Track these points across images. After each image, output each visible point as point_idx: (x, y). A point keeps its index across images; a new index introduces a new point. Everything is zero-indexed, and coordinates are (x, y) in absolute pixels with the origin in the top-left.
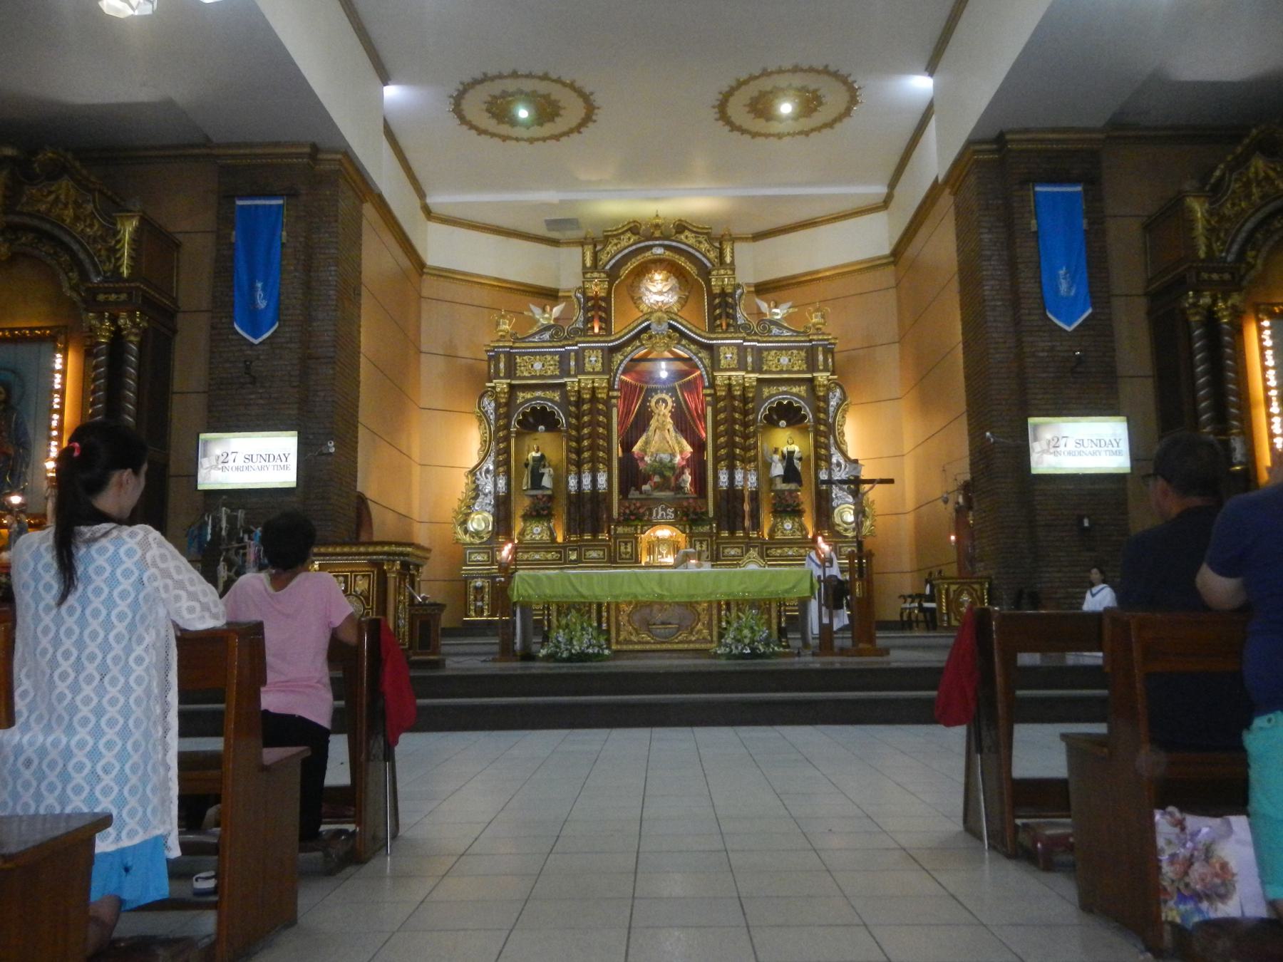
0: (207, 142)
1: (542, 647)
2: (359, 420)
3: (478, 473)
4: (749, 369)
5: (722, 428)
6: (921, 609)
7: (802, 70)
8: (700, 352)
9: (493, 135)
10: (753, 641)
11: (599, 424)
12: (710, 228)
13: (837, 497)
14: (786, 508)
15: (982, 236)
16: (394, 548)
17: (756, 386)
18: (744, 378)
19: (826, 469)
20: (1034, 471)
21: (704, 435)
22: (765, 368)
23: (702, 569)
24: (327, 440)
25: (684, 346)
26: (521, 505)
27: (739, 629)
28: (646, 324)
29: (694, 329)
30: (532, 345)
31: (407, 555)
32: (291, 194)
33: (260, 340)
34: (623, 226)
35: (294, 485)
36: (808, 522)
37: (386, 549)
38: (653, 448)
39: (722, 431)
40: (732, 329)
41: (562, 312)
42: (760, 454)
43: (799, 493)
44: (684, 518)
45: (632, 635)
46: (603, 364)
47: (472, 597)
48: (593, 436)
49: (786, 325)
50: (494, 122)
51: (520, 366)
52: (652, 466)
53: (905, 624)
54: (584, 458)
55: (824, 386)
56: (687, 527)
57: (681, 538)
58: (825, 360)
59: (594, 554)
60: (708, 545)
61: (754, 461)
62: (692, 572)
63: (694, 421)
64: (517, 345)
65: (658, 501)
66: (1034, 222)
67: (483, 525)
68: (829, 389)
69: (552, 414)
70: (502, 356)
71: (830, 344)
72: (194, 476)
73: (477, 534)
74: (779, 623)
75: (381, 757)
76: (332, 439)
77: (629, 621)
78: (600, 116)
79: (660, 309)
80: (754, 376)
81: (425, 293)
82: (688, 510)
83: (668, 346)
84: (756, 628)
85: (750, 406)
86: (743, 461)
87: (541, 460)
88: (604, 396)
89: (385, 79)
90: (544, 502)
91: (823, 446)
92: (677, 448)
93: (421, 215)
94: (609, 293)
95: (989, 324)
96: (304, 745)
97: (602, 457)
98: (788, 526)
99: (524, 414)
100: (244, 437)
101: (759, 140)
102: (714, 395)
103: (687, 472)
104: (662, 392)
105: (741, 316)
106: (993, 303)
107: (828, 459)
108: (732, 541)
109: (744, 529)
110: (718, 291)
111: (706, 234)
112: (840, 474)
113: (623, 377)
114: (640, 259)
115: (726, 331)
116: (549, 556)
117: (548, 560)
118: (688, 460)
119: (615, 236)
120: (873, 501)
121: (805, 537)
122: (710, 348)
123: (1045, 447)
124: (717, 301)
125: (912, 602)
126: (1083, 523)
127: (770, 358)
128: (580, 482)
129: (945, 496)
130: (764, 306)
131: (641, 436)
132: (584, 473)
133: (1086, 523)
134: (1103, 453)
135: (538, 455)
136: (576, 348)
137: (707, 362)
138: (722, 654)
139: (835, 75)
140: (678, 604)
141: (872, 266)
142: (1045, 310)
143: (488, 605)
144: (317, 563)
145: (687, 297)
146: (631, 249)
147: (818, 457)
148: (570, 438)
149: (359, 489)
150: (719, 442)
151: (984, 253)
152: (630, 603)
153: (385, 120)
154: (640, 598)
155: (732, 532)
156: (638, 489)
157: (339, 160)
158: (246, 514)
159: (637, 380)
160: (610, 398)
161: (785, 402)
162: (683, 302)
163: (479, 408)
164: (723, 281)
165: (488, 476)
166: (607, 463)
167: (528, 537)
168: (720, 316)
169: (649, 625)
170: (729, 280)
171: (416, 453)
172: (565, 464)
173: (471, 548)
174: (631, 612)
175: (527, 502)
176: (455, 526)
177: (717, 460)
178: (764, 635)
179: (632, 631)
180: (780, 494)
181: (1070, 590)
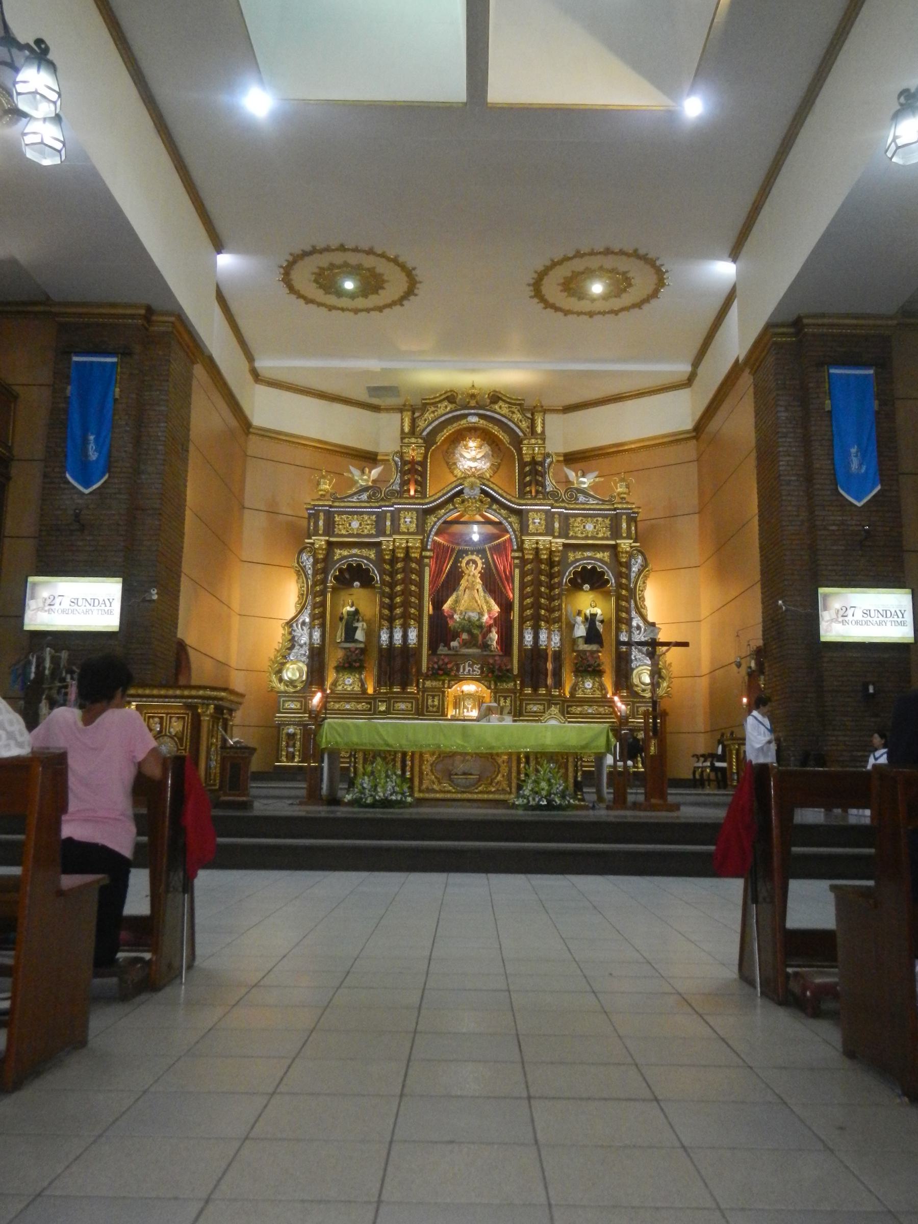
0: (47, 301)
1: (348, 793)
2: (183, 570)
3: (294, 625)
4: (556, 534)
5: (529, 589)
6: (713, 767)
7: (613, 253)
8: (510, 518)
9: (320, 304)
10: (549, 794)
11: (412, 582)
12: (523, 400)
13: (636, 659)
15: (779, 414)
16: (209, 693)
17: (562, 551)
18: (551, 543)
19: (626, 632)
20: (823, 639)
21: (511, 596)
22: (571, 533)
23: (503, 723)
24: (150, 588)
25: (495, 510)
26: (334, 657)
27: (536, 782)
28: (459, 488)
29: (505, 495)
30: (351, 504)
31: (221, 699)
32: (125, 353)
34: (441, 395)
35: (116, 629)
36: (608, 681)
37: (201, 693)
38: (463, 606)
39: (528, 593)
41: (380, 475)
42: (564, 617)
43: (600, 654)
44: (490, 675)
45: (434, 783)
46: (417, 525)
47: (284, 743)
48: (406, 593)
49: (592, 493)
50: (321, 292)
51: (338, 525)
52: (460, 623)
53: (697, 782)
54: (397, 614)
55: (627, 552)
56: (493, 682)
57: (486, 693)
58: (629, 528)
59: (402, 706)
60: (511, 701)
61: (558, 622)
62: (493, 726)
63: (503, 584)
64: (336, 504)
65: (466, 657)
66: (828, 402)
67: (298, 675)
68: (631, 556)
69: (367, 571)
70: (322, 514)
71: (634, 513)
72: (20, 616)
73: (291, 683)
74: (576, 777)
75: (180, 889)
76: (155, 587)
77: (432, 771)
78: (421, 290)
79: (473, 475)
80: (561, 541)
81: (249, 452)
82: (494, 667)
83: (480, 510)
84: (553, 781)
85: (556, 569)
86: (547, 622)
89: (219, 247)
90: (357, 654)
91: (624, 609)
92: (485, 608)
93: (249, 378)
94: (425, 457)
95: (784, 498)
96: (103, 873)
97: (413, 614)
98: (589, 685)
99: (341, 570)
100: (72, 582)
101: (570, 317)
102: (522, 559)
103: (494, 630)
104: (472, 554)
105: (550, 483)
106: (788, 478)
107: (629, 621)
109: (546, 686)
110: (529, 460)
111: (520, 405)
112: (639, 636)
113: (436, 538)
114: (454, 427)
115: (535, 498)
116: (359, 707)
117: (359, 711)
118: (495, 619)
119: (433, 404)
120: (671, 663)
121: (605, 696)
122: (519, 513)
123: (834, 616)
124: (527, 469)
125: (705, 761)
126: (868, 690)
127: (576, 524)
128: (391, 637)
129: (738, 660)
130: (572, 475)
131: (451, 594)
132: (396, 628)
133: (871, 690)
134: (889, 624)
135: (353, 609)
136: (392, 509)
137: (516, 526)
138: (519, 805)
139: (644, 258)
140: (479, 755)
141: (676, 440)
142: (837, 485)
143: (299, 751)
144: (134, 703)
145: (499, 464)
146: (447, 416)
147: (619, 620)
148: (383, 594)
149: (180, 635)
150: (525, 603)
151: (780, 430)
152: (433, 754)
153: (218, 286)
154: (443, 749)
155: (535, 689)
156: (447, 645)
157: (172, 323)
158: (69, 655)
159: (448, 541)
160: (422, 557)
161: (589, 567)
162: (495, 468)
163: (298, 563)
164: (534, 450)
165: (304, 628)
166: (417, 619)
167: (340, 688)
168: (529, 484)
169: (450, 775)
170: (539, 449)
172: (378, 619)
173: (285, 696)
174: (434, 761)
175: (340, 654)
176: (270, 675)
177: (522, 621)
178: (561, 788)
179: (435, 780)
181: (855, 753)
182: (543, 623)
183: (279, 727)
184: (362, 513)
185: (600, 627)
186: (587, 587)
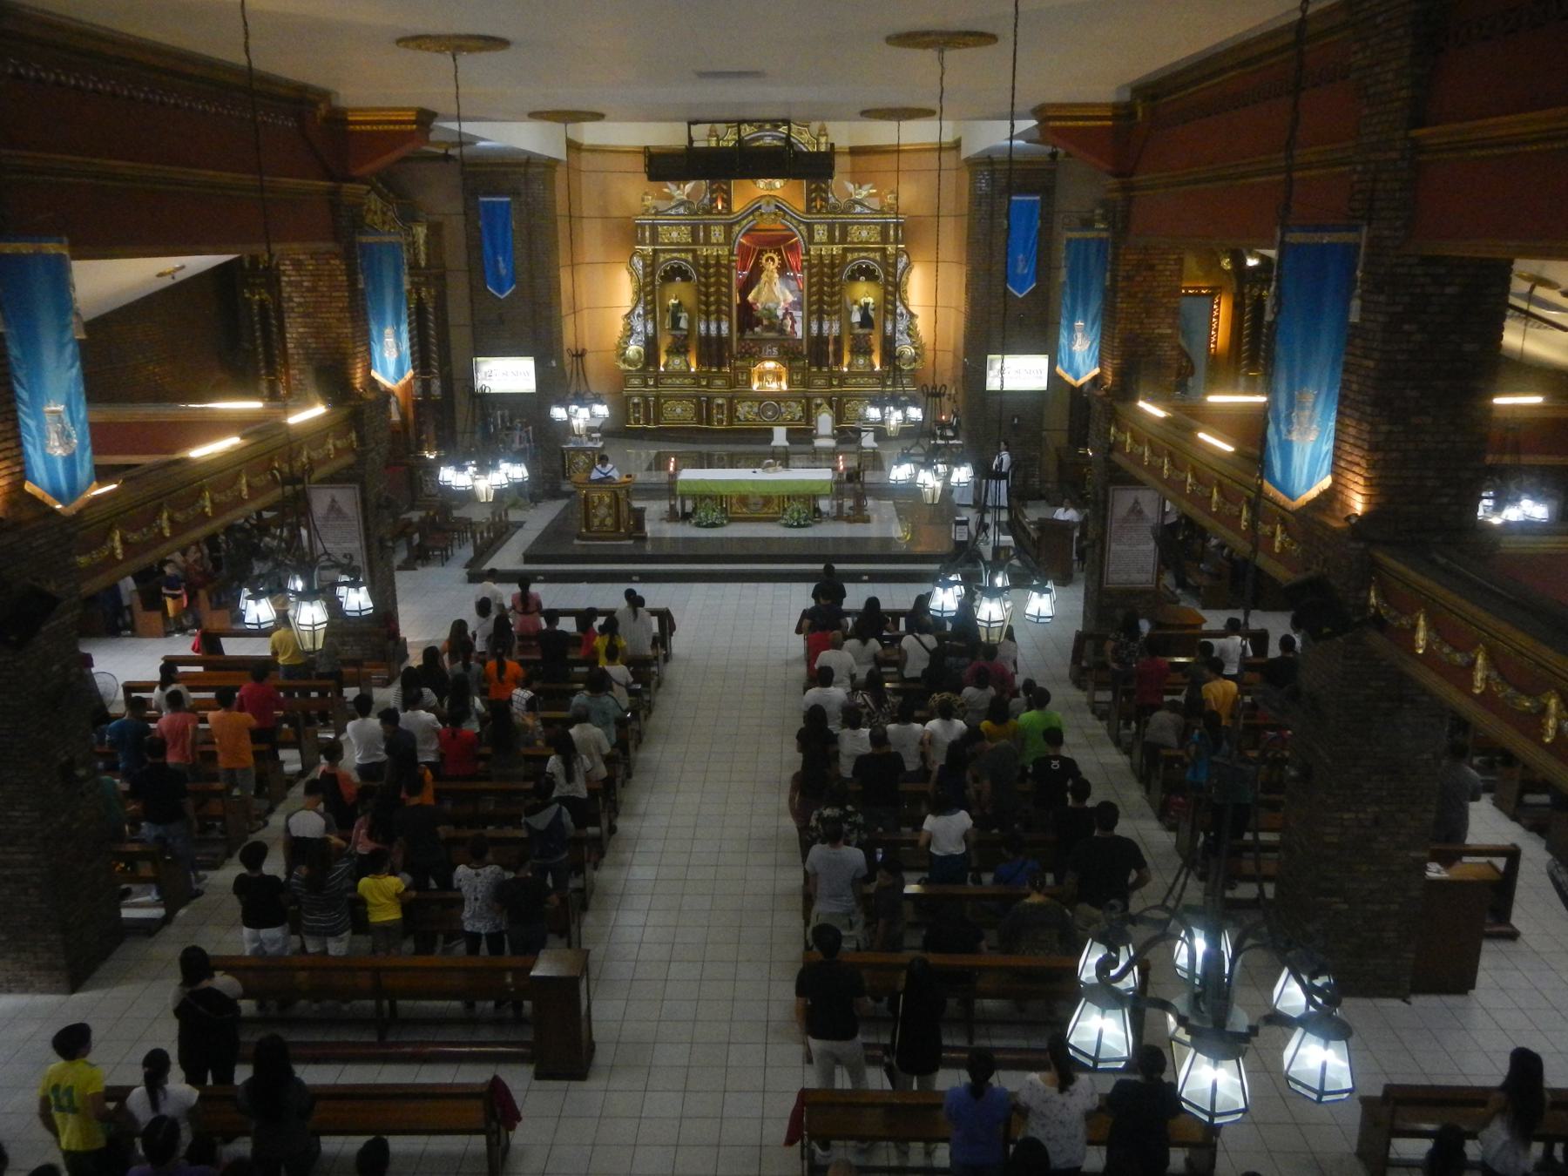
5: (814, 289)
10: (799, 518)
14: (860, 348)
20: (987, 389)
22: (849, 239)
26: (665, 342)
32: (515, 193)
38: (763, 299)
41: (693, 188)
48: (718, 292)
59: (719, 382)
66: (1006, 222)
68: (897, 256)
69: (686, 272)
70: (647, 227)
85: (836, 270)
86: (828, 315)
88: (726, 262)
99: (665, 272)
107: (894, 313)
108: (819, 374)
115: (819, 212)
128: (708, 328)
131: (752, 289)
133: (1016, 421)
135: (676, 302)
137: (805, 234)
140: (761, 497)
147: (886, 311)
148: (699, 292)
156: (752, 330)
160: (730, 261)
171: (584, 300)
180: (856, 338)
183: (629, 397)
184: (679, 225)
185: (872, 314)
186: (862, 278)
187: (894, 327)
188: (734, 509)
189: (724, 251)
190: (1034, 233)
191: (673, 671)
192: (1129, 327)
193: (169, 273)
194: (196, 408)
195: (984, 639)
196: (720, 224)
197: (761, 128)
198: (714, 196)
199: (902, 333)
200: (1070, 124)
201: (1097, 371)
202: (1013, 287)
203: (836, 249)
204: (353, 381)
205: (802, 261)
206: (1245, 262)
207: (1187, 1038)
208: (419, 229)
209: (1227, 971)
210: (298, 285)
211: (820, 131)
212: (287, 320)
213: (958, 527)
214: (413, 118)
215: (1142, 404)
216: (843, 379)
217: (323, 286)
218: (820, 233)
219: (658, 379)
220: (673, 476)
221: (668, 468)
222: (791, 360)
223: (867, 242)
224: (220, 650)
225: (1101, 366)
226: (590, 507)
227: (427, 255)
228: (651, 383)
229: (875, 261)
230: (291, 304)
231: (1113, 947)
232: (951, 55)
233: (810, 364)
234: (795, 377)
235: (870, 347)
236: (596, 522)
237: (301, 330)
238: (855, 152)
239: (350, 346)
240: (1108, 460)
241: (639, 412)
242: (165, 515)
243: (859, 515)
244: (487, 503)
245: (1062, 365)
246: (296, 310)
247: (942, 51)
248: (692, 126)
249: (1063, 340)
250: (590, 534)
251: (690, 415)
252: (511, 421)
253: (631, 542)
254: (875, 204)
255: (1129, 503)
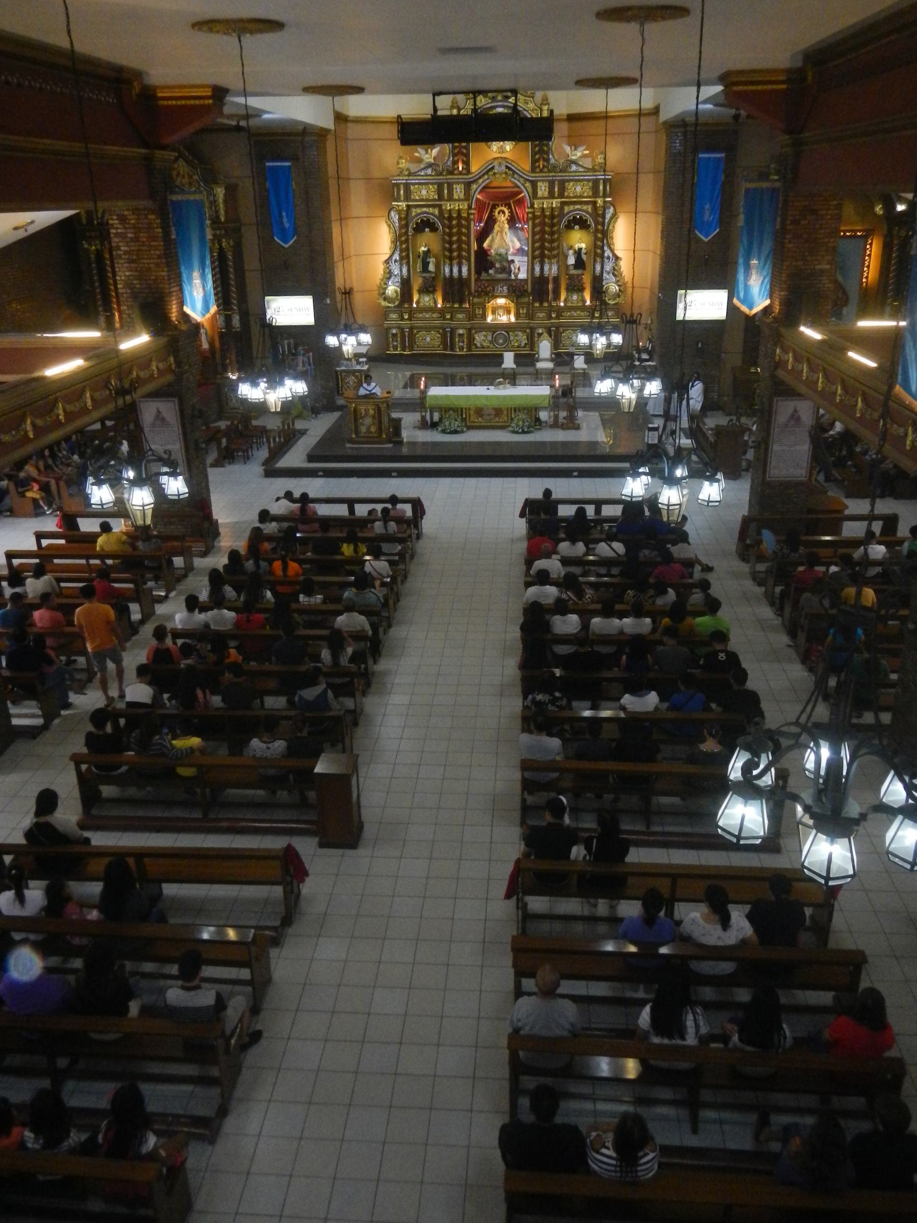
4: (556, 195)
5: (537, 237)
22: (566, 194)
26: (416, 284)
32: (294, 158)
33: (288, 245)
38: (495, 246)
40: (546, 170)
41: (439, 152)
48: (459, 241)
59: (460, 316)
64: (411, 178)
68: (605, 208)
69: (434, 223)
70: (402, 186)
85: (556, 221)
86: (549, 258)
87: (427, 253)
92: (511, 246)
99: (417, 224)
107: (602, 256)
109: (548, 301)
115: (541, 171)
116: (434, 315)
127: (570, 187)
128: (451, 270)
133: (700, 345)
135: (426, 249)
137: (530, 190)
147: (596, 254)
148: (444, 241)
155: (541, 304)
156: (487, 272)
167: (422, 304)
168: (538, 160)
171: (351, 249)
180: (571, 277)
182: (546, 260)
185: (584, 257)
186: (577, 227)
187: (602, 268)
188: (472, 418)
189: (464, 206)
190: (718, 186)
191: (422, 546)
192: (794, 263)
193: (23, 227)
194: (47, 338)
195: (665, 519)
196: (458, 183)
197: (494, 99)
198: (456, 159)
199: (608, 273)
200: (751, 88)
201: (768, 302)
202: (701, 232)
203: (555, 203)
204: (171, 315)
205: (528, 213)
206: (895, 207)
207: (811, 822)
208: (219, 190)
209: (844, 773)
210: (123, 236)
211: (543, 100)
212: (116, 265)
213: (650, 433)
214: (210, 94)
215: (803, 329)
216: (560, 312)
217: (143, 236)
218: (543, 189)
219: (411, 312)
220: (424, 393)
221: (418, 386)
222: (518, 297)
223: (581, 197)
224: (76, 527)
225: (771, 297)
226: (359, 417)
227: (226, 212)
228: (406, 317)
229: (587, 212)
230: (120, 252)
231: (756, 754)
232: (650, 27)
233: (534, 301)
234: (521, 311)
235: (582, 285)
236: (363, 429)
237: (127, 274)
238: (572, 118)
239: (167, 286)
240: (773, 376)
241: (397, 341)
242: (29, 422)
243: (572, 424)
244: (276, 413)
245: (739, 299)
246: (123, 257)
247: (642, 24)
248: (436, 98)
249: (741, 277)
250: (357, 439)
251: (437, 342)
252: (296, 350)
253: (390, 445)
254: (588, 163)
255: (790, 411)
